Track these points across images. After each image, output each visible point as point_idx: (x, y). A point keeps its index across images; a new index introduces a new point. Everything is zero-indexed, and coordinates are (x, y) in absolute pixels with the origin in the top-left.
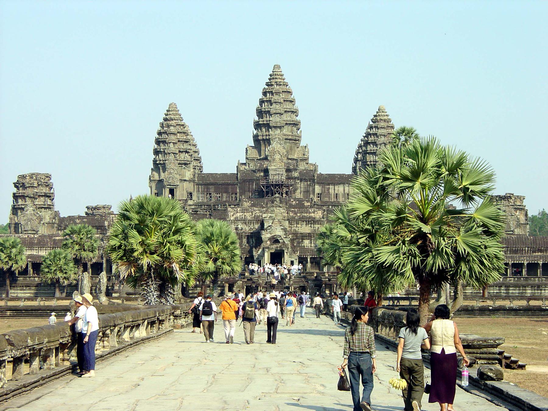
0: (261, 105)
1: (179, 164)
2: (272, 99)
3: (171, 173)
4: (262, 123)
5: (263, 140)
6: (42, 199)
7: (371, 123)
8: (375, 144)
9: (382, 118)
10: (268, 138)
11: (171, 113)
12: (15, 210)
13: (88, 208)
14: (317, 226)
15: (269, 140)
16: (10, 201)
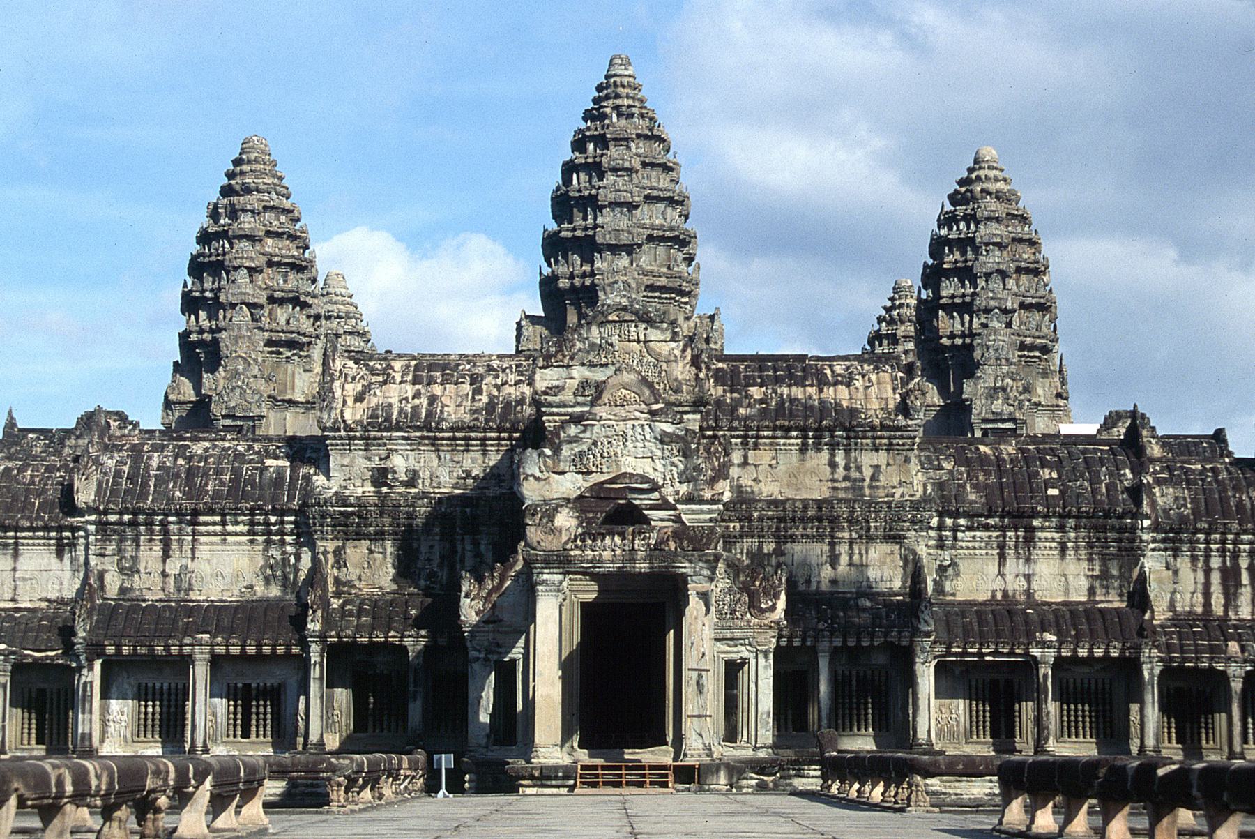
0: (567, 181)
1: (269, 343)
2: (604, 160)
3: (236, 374)
4: (570, 234)
7: (949, 207)
8: (965, 273)
9: (992, 187)
10: (588, 282)
11: (245, 168)
14: (868, 460)
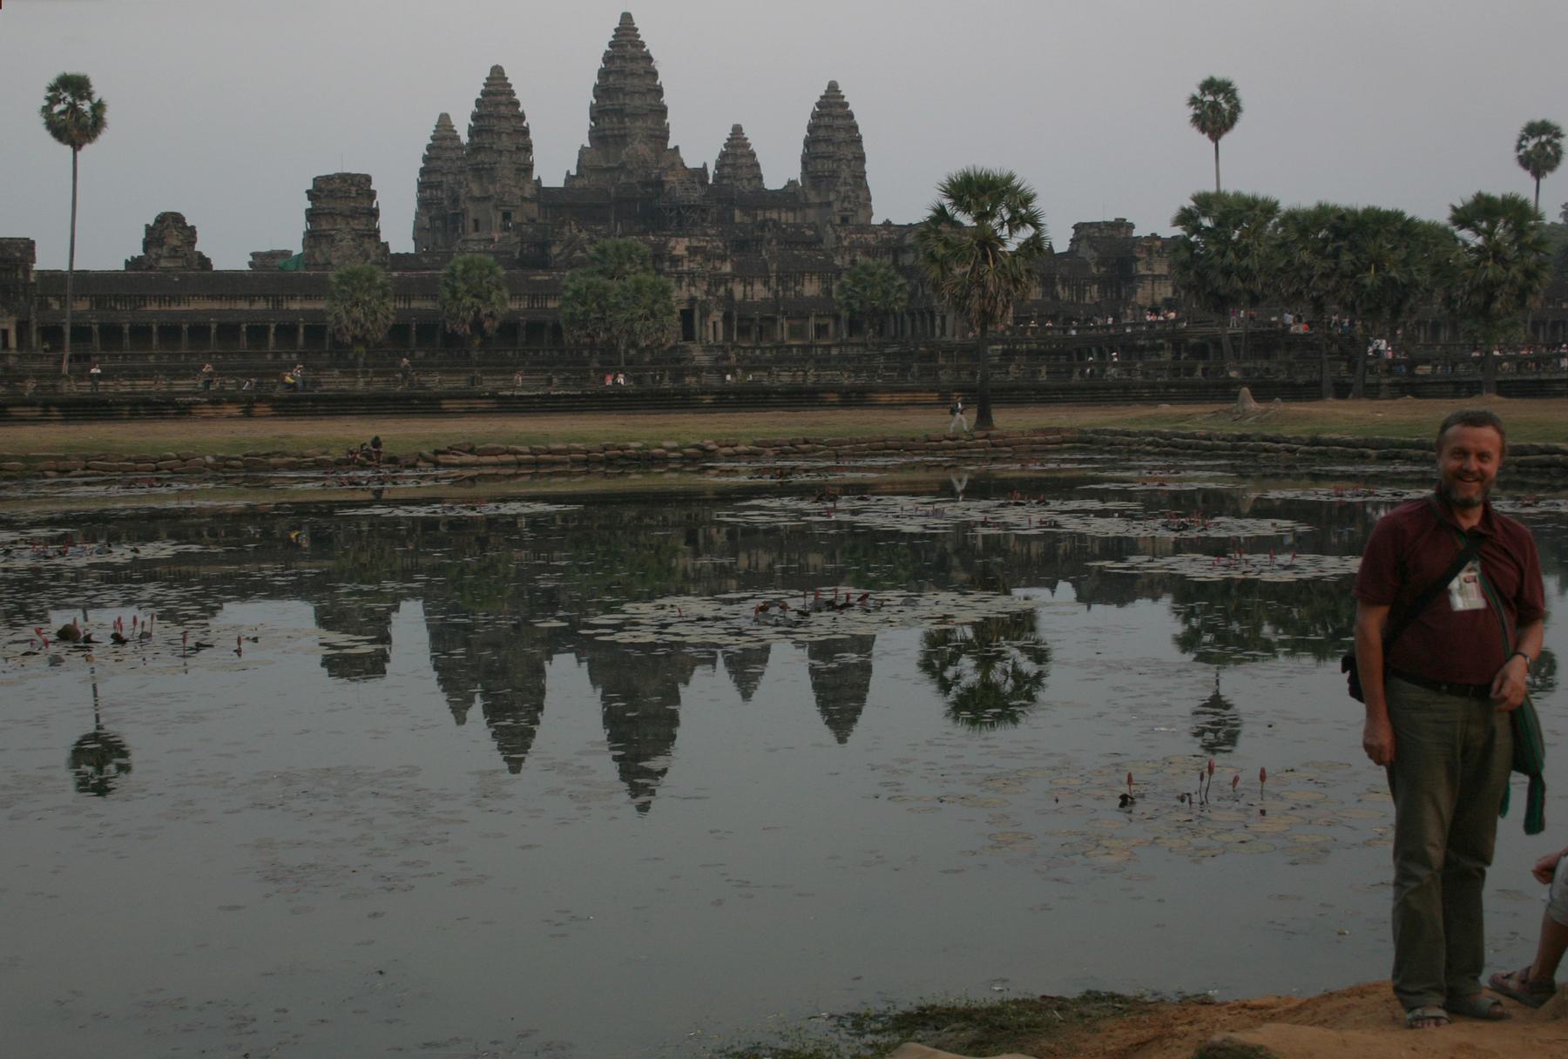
5: (614, 136)
6: (364, 220)
8: (828, 141)
12: (311, 237)
13: (254, 255)
15: (624, 136)
16: (300, 225)
